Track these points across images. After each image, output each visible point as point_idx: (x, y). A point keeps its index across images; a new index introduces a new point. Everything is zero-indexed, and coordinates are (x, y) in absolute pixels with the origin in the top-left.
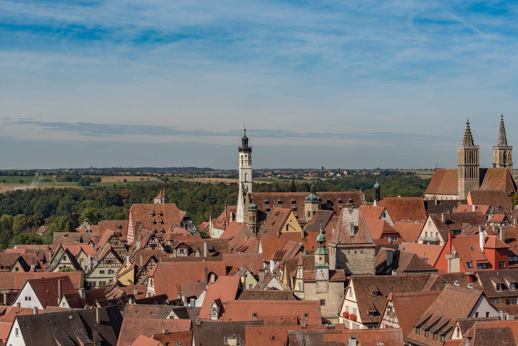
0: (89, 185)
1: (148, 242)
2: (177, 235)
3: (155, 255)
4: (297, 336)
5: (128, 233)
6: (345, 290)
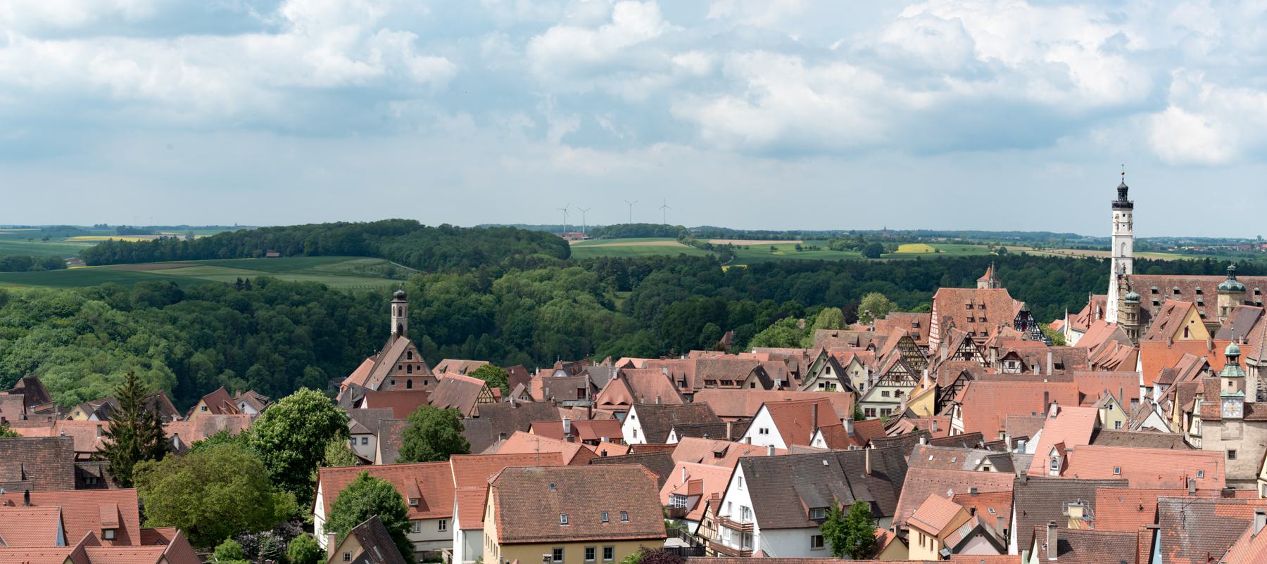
2: (1007, 338)
4: (1172, 506)
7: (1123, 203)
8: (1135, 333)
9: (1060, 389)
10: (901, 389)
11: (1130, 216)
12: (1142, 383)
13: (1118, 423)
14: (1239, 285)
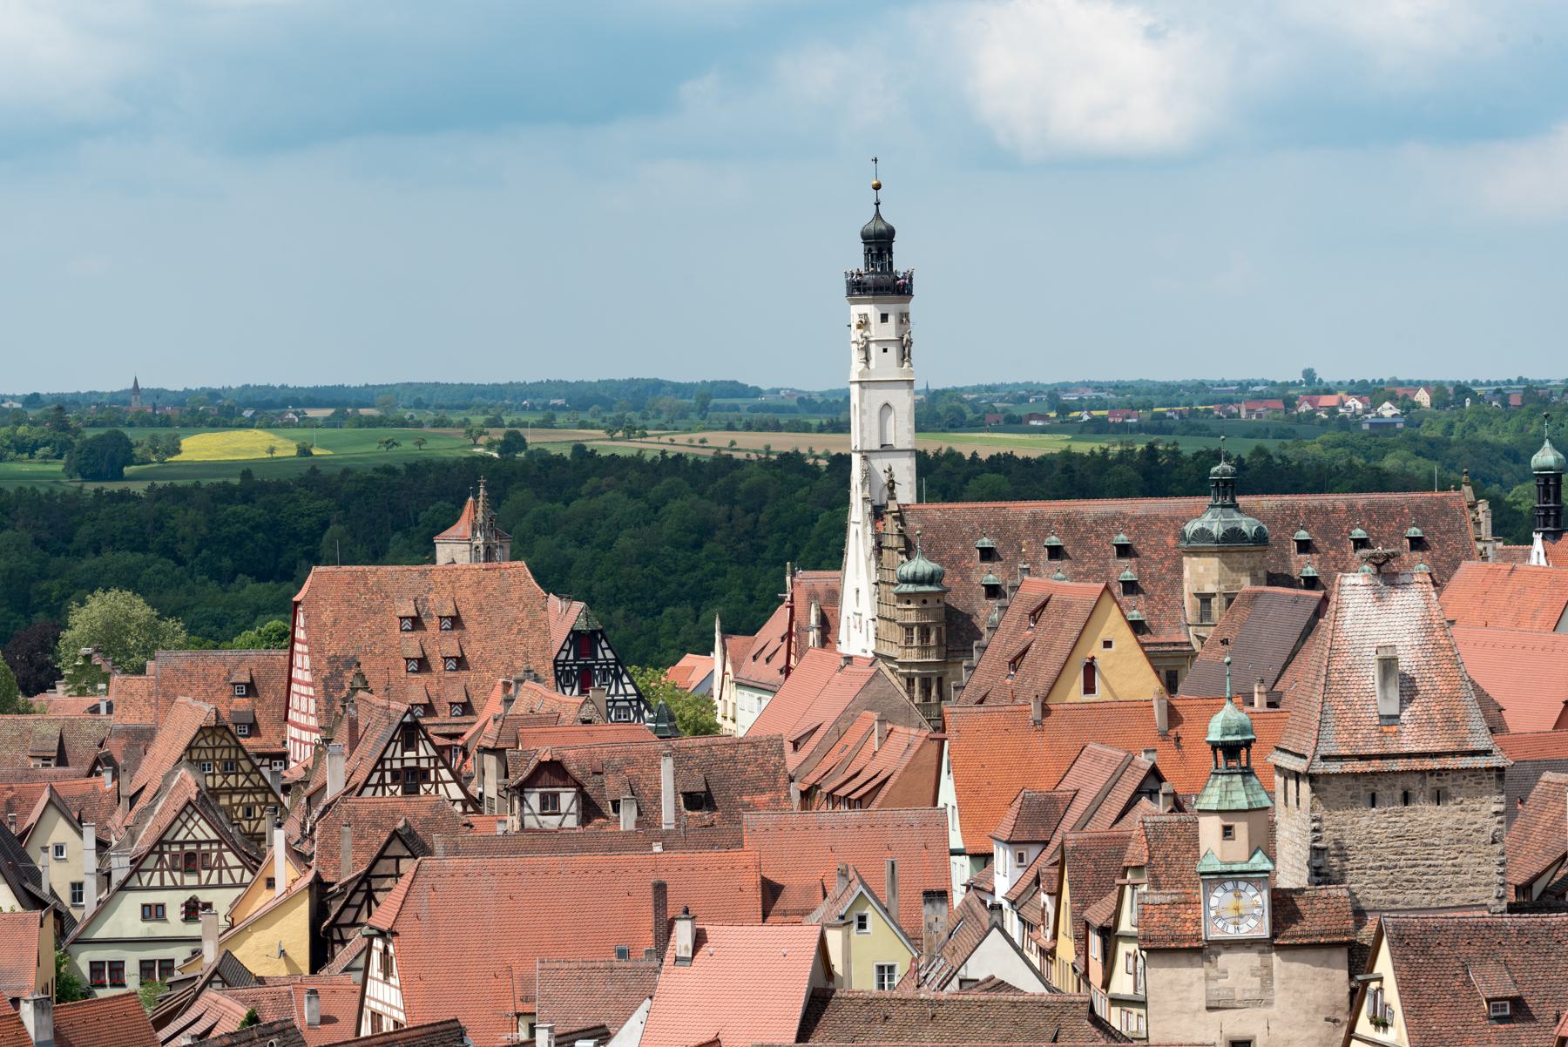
0: (119, 476)
1: (381, 760)
3: (416, 826)
5: (292, 716)
6: (1353, 992)
7: (881, 278)
8: (931, 686)
9: (698, 872)
10: (204, 896)
11: (904, 318)
12: (956, 841)
13: (885, 971)
14: (1247, 525)
